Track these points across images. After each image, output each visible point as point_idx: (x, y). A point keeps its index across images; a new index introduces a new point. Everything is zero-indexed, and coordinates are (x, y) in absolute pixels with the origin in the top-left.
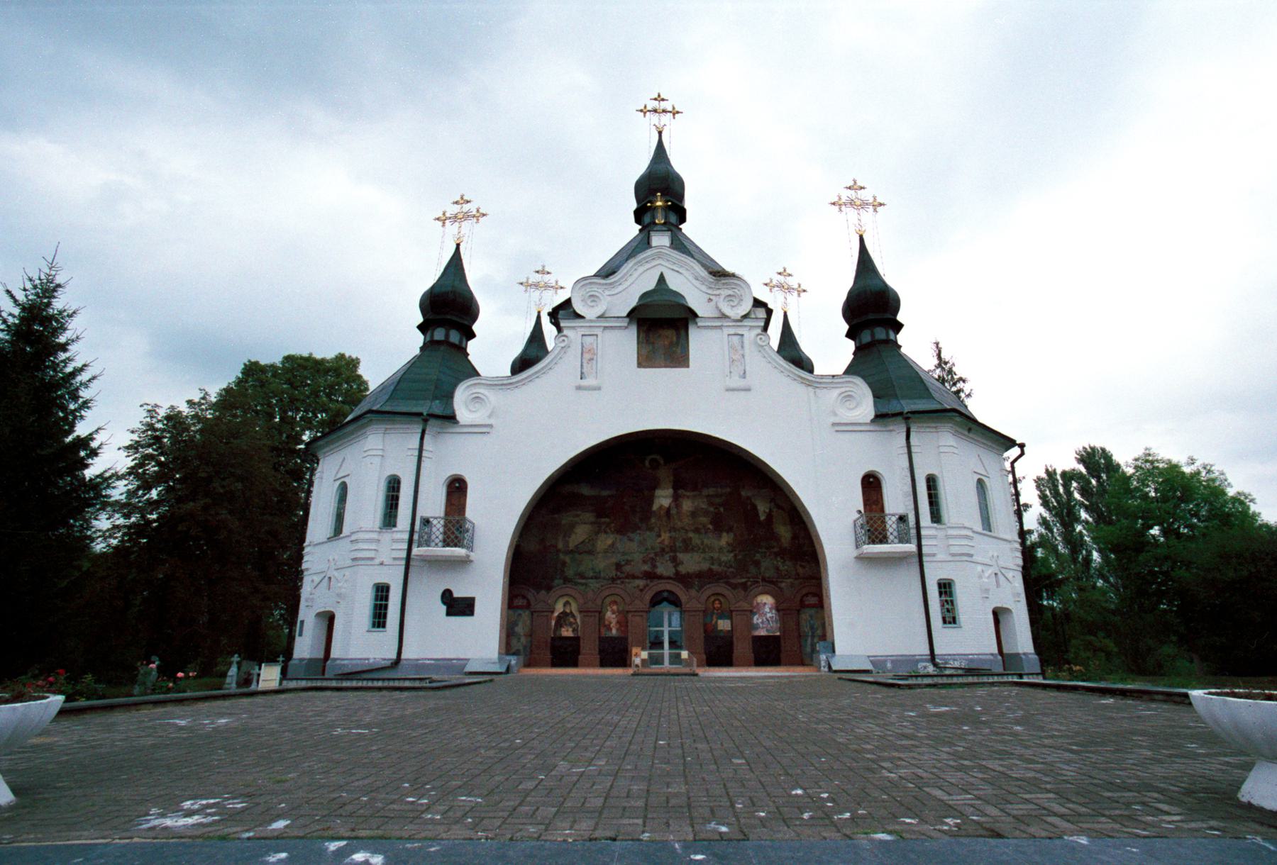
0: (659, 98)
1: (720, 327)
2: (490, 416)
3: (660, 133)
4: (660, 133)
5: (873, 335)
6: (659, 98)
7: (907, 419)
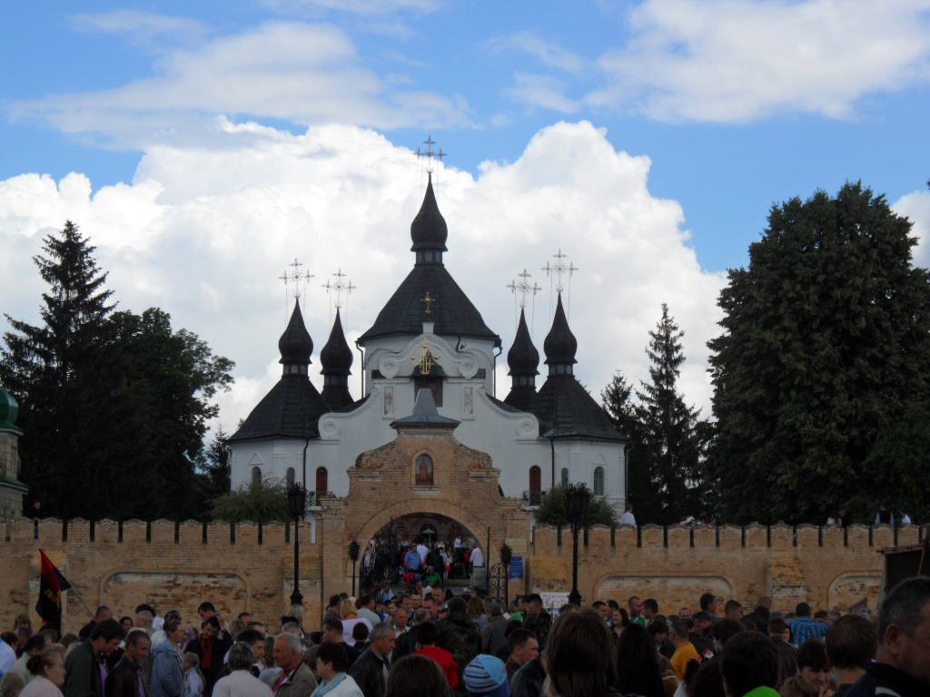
0: (429, 142)
1: (460, 383)
2: (340, 433)
3: (430, 177)
4: (430, 177)
5: (556, 371)
6: (429, 142)
7: (552, 441)
